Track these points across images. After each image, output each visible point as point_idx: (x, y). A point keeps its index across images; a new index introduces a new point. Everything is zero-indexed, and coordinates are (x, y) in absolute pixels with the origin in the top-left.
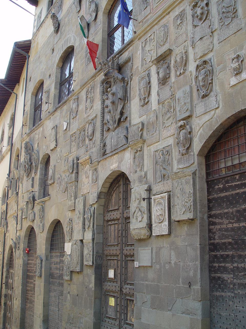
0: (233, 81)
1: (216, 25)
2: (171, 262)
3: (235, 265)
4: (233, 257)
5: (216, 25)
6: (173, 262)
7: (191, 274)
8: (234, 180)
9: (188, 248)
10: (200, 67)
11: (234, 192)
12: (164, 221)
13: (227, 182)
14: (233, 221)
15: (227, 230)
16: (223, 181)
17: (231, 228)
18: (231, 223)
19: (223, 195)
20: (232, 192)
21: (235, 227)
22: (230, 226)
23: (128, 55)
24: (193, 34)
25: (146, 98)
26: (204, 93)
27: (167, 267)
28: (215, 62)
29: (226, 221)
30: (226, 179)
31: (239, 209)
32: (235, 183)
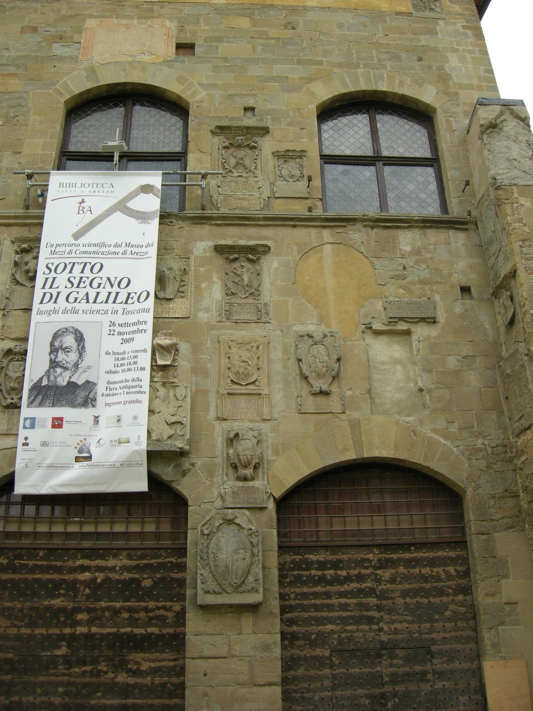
8: (35, 557)
10: (15, 355)
11: (30, 577)
13: (19, 557)
14: (19, 624)
16: (11, 554)
17: (15, 635)
18: (15, 626)
20: (26, 576)
21: (23, 634)
22: (14, 631)
24: (10, 293)
26: (12, 401)
30: (17, 552)
31: (36, 605)
32: (36, 563)
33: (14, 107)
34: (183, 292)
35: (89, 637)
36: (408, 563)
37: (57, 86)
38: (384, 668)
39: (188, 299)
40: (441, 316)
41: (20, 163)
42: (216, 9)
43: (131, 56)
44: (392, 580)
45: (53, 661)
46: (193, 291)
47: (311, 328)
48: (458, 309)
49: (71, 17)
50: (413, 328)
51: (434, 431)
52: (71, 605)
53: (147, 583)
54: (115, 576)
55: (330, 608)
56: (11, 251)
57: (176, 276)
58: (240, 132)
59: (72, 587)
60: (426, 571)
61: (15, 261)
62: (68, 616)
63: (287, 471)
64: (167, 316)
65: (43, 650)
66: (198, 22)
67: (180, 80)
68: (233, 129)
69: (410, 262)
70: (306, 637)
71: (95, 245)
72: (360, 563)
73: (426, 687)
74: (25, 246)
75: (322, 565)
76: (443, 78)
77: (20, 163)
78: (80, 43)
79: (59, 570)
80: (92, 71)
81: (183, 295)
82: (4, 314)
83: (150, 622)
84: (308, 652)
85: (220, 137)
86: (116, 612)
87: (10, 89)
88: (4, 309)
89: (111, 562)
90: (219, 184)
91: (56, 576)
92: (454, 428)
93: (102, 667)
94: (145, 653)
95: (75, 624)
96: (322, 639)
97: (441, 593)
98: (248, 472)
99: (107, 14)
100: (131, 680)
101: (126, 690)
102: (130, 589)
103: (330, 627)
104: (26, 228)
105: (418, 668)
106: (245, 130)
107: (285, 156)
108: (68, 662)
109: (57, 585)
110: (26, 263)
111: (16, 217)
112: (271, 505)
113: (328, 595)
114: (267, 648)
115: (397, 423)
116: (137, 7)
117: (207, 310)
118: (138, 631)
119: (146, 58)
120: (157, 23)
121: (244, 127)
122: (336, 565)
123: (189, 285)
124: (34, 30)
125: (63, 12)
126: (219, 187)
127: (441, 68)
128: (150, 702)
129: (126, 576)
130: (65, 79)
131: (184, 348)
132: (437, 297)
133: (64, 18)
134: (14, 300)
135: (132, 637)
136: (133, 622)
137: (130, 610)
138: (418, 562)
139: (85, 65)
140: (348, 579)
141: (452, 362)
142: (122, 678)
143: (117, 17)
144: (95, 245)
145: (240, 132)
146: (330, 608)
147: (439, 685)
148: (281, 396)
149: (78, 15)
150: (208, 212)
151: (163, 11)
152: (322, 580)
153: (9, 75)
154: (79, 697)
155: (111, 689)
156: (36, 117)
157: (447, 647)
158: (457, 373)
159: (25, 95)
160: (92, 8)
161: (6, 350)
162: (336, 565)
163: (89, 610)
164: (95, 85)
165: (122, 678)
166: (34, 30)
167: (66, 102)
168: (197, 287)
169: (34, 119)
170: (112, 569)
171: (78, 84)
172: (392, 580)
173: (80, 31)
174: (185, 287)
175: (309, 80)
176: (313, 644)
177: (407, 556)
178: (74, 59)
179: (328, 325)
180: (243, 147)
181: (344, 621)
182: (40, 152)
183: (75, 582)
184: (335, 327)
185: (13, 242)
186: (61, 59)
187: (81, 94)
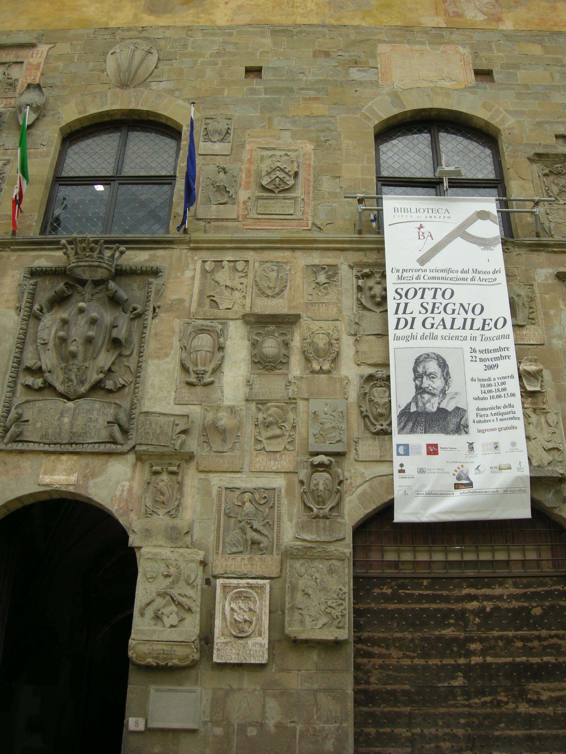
2: (267, 721)
3: (418, 730)
4: (410, 716)
6: (271, 723)
8: (419, 586)
9: (321, 696)
10: (377, 380)
11: (417, 606)
12: (252, 635)
14: (412, 654)
15: (399, 668)
16: (394, 583)
17: (408, 666)
18: (405, 656)
19: (391, 607)
20: (413, 606)
21: (417, 665)
22: (408, 662)
23: (146, 261)
24: (359, 318)
25: (207, 372)
26: (382, 427)
27: (252, 732)
29: (394, 652)
30: (400, 581)
31: (427, 635)
32: (421, 592)
33: (323, 131)
34: (533, 319)
35: (485, 667)
37: (363, 111)
39: (539, 326)
41: (341, 188)
42: (505, 36)
43: (431, 81)
45: (451, 691)
46: (543, 318)
49: (361, 42)
53: (537, 611)
54: (504, 605)
56: (351, 276)
57: (525, 303)
58: (558, 160)
59: (461, 615)
61: (359, 286)
62: (461, 646)
64: (522, 342)
65: (440, 681)
66: (491, 49)
68: (551, 156)
71: (442, 271)
74: (366, 270)
77: (341, 188)
78: (377, 68)
79: (446, 599)
80: (395, 96)
81: (534, 322)
82: (356, 340)
83: (544, 651)
85: (538, 164)
86: (509, 641)
87: (315, 113)
88: (356, 335)
89: (498, 591)
90: (548, 212)
91: (443, 606)
93: (502, 697)
94: (543, 683)
95: (469, 654)
99: (397, 39)
100: (533, 711)
101: (529, 721)
102: (520, 618)
104: (362, 253)
106: (562, 158)
109: (446, 614)
110: (371, 289)
111: (351, 242)
116: (426, 32)
118: (534, 660)
119: (447, 84)
120: (450, 48)
121: (562, 155)
123: (538, 312)
124: (327, 54)
125: (353, 37)
126: (548, 214)
128: (554, 732)
129: (515, 604)
130: (370, 104)
131: (546, 374)
133: (354, 43)
134: (364, 325)
135: (528, 666)
136: (528, 651)
137: (523, 639)
139: (386, 90)
142: (523, 708)
143: (409, 43)
144: (442, 271)
145: (558, 160)
149: (369, 40)
150: (545, 239)
151: (453, 37)
153: (310, 99)
154: (482, 728)
155: (514, 719)
156: (348, 141)
159: (332, 120)
160: (381, 33)
161: (366, 376)
163: (481, 640)
164: (402, 111)
165: (523, 708)
166: (327, 54)
167: (375, 127)
168: (546, 314)
169: (346, 143)
170: (500, 598)
173: (374, 56)
174: (534, 314)
178: (375, 84)
180: (563, 175)
182: (360, 176)
183: (464, 611)
185: (351, 267)
186: (361, 83)
187: (389, 119)
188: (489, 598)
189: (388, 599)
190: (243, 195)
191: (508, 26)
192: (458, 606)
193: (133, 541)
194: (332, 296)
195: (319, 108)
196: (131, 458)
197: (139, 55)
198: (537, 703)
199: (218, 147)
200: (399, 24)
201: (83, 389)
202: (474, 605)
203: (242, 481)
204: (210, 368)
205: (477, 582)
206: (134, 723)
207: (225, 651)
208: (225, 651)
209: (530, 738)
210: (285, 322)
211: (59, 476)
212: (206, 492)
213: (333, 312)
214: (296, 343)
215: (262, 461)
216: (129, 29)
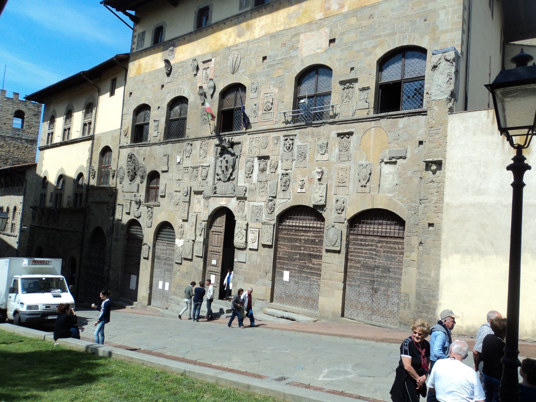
0: (299, 190)
1: (295, 157)
4: (287, 263)
5: (295, 157)
6: (258, 262)
7: (268, 268)
15: (286, 252)
19: (286, 236)
27: (255, 264)
28: (291, 175)
29: (286, 248)
35: (304, 254)
36: (387, 242)
38: (375, 273)
40: (408, 155)
42: (344, 16)
43: (314, 51)
44: (381, 247)
45: (296, 259)
47: (364, 162)
48: (416, 151)
50: (397, 160)
51: (398, 200)
52: (300, 245)
54: (310, 238)
55: (362, 253)
59: (300, 240)
60: (392, 245)
63: (351, 212)
67: (330, 59)
69: (401, 132)
70: (355, 260)
72: (372, 241)
73: (386, 281)
75: (361, 240)
76: (435, 29)
79: (297, 235)
84: (355, 265)
86: (310, 248)
89: (309, 234)
92: (405, 199)
95: (301, 250)
96: (359, 262)
97: (395, 253)
98: (340, 212)
100: (313, 266)
101: (311, 268)
103: (361, 259)
105: (385, 275)
107: (363, 89)
108: (299, 260)
109: (297, 239)
112: (346, 221)
113: (362, 249)
114: (341, 262)
115: (386, 197)
117: (334, 157)
118: (314, 253)
119: (319, 51)
122: (365, 240)
127: (434, 23)
129: (312, 238)
132: (409, 147)
135: (313, 255)
136: (313, 251)
137: (313, 248)
138: (390, 242)
140: (368, 245)
141: (409, 174)
142: (310, 265)
146: (362, 253)
147: (390, 281)
148: (353, 186)
151: (325, 23)
152: (361, 245)
155: (308, 267)
157: (395, 270)
158: (411, 178)
162: (365, 240)
163: (304, 247)
165: (310, 265)
168: (331, 149)
170: (309, 236)
171: (298, 69)
172: (381, 247)
175: (375, 47)
176: (356, 263)
177: (387, 240)
179: (369, 161)
181: (366, 257)
183: (301, 239)
184: (371, 162)
188: (307, 236)
189: (285, 234)
190: (260, 113)
191: (345, 10)
192: (300, 238)
193: (236, 219)
194: (278, 148)
195: (281, 72)
196: (236, 198)
197: (235, 59)
198: (313, 264)
199: (255, 95)
200: (308, 21)
201: (226, 180)
202: (303, 237)
203: (256, 204)
204: (250, 172)
205: (305, 231)
206: (235, 260)
207: (250, 246)
208: (250, 246)
209: (310, 272)
210: (267, 158)
211: (223, 202)
212: (249, 206)
213: (277, 153)
214: (269, 164)
215: (260, 198)
216: (233, 46)
